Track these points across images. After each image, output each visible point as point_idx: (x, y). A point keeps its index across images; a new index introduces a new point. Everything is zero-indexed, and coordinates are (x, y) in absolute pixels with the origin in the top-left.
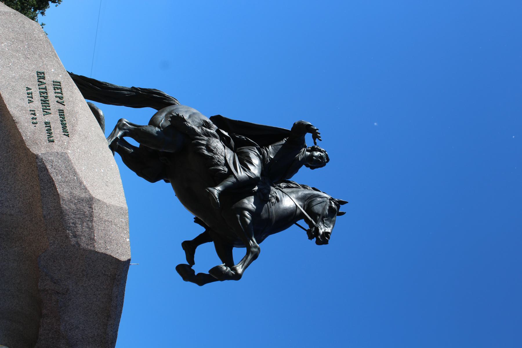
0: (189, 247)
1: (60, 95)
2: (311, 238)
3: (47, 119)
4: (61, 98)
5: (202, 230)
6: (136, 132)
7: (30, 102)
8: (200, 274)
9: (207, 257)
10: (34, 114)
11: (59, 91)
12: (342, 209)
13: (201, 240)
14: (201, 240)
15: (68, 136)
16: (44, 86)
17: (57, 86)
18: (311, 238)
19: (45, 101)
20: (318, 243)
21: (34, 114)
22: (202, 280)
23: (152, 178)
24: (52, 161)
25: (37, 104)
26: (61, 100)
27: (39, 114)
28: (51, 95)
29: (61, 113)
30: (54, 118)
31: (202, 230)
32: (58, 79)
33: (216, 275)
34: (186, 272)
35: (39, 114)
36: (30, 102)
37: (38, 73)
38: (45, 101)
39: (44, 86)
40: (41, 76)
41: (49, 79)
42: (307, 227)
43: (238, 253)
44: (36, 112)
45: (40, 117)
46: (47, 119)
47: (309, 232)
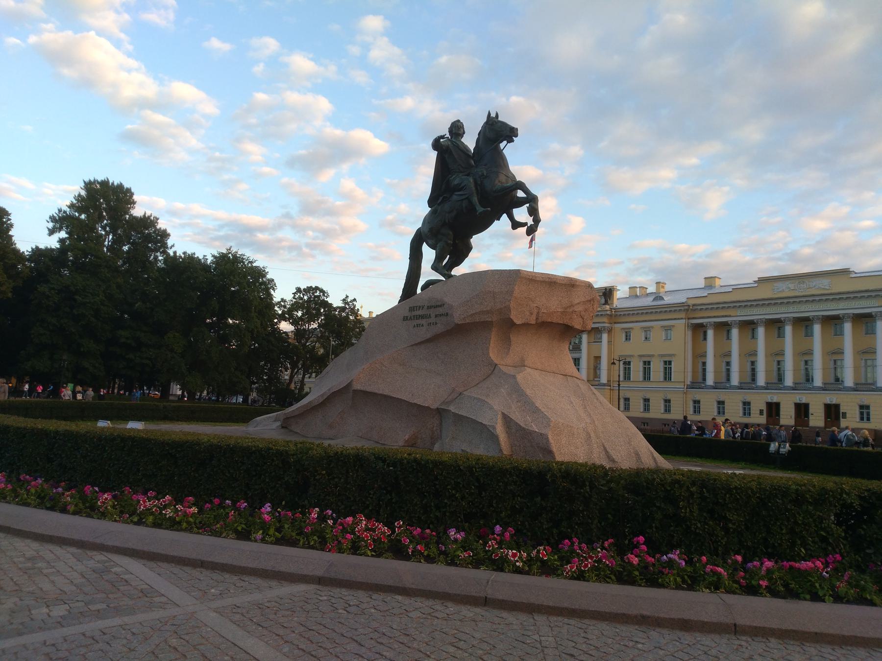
0: (516, 225)
2: (513, 141)
3: (433, 315)
5: (505, 215)
6: (439, 258)
9: (521, 214)
12: (493, 115)
13: (511, 217)
14: (511, 217)
17: (412, 309)
18: (513, 141)
19: (422, 317)
20: (516, 136)
22: (537, 221)
23: (469, 248)
25: (423, 322)
26: (421, 307)
30: (432, 312)
31: (505, 215)
33: (533, 212)
38: (422, 317)
40: (405, 319)
42: (505, 142)
43: (520, 194)
45: (433, 320)
46: (433, 315)
47: (508, 142)
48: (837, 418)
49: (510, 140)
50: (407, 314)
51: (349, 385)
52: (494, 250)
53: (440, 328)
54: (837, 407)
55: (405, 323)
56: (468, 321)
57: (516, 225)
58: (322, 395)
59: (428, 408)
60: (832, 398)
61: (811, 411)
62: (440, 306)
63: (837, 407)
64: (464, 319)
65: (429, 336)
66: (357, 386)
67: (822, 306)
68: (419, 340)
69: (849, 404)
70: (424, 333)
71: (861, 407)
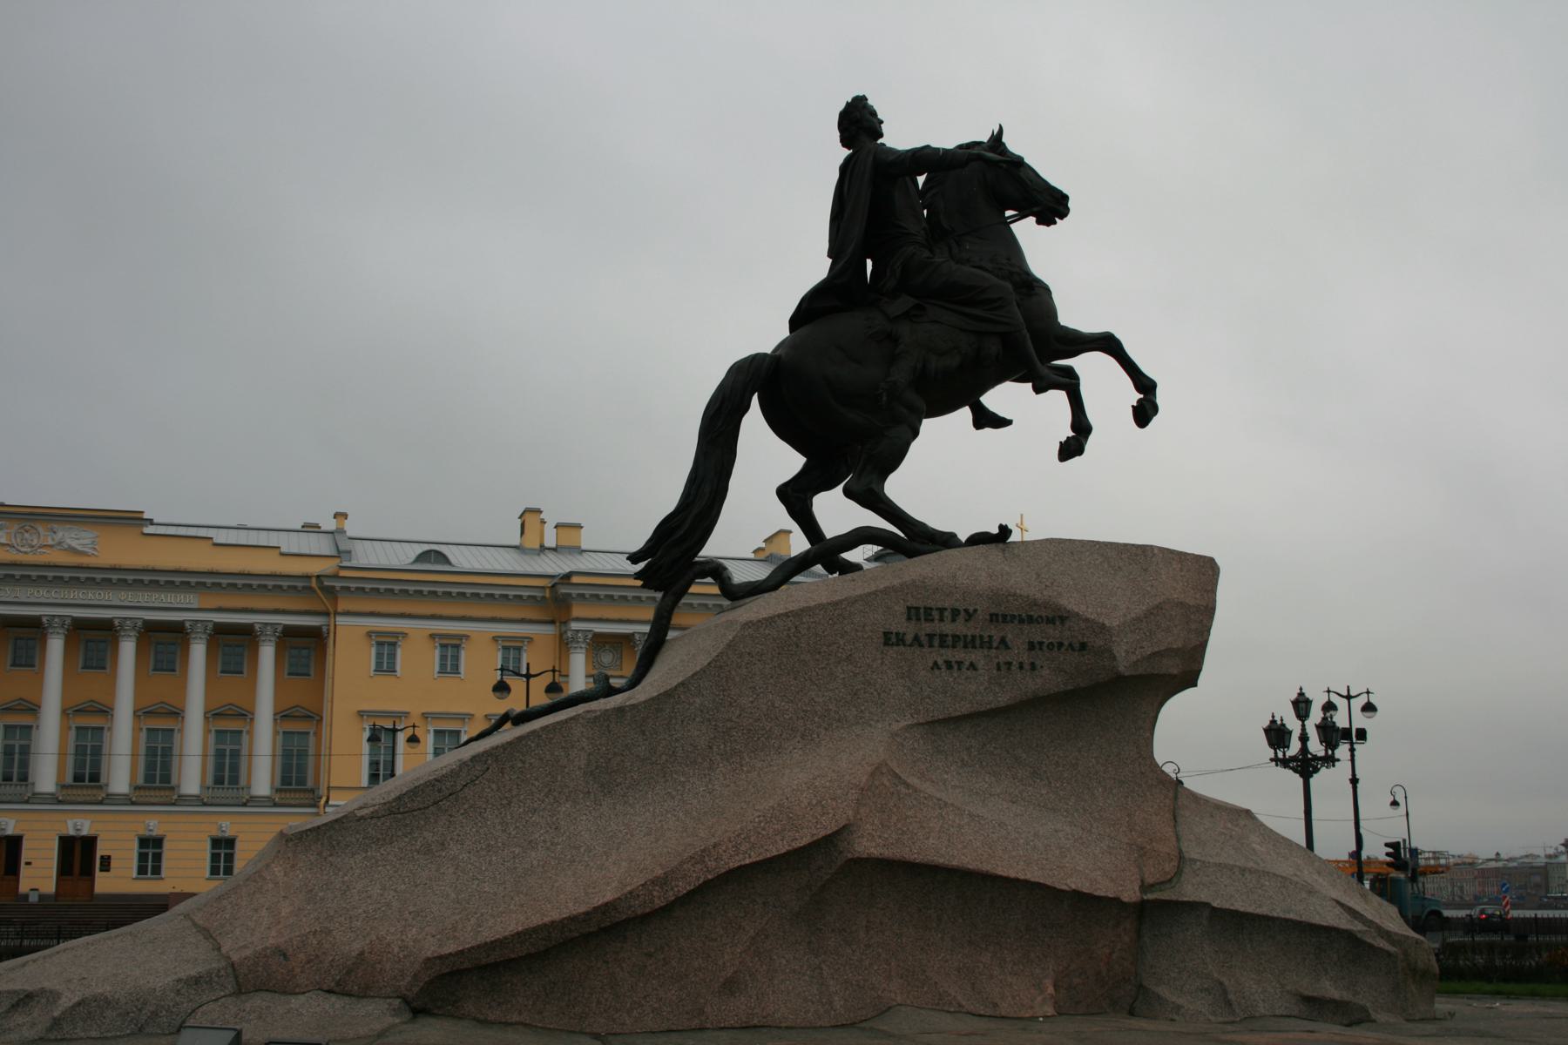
1: (946, 614)
4: (955, 613)
7: (972, 666)
8: (1073, 427)
10: (1009, 664)
11: (936, 614)
15: (1063, 619)
16: (924, 639)
21: (1009, 664)
24: (1127, 652)
25: (976, 656)
27: (1004, 657)
28: (948, 628)
29: (994, 618)
32: (900, 608)
34: (1071, 449)
35: (1004, 657)
36: (972, 666)
37: (886, 644)
38: (970, 643)
39: (924, 639)
41: (899, 624)
44: (1001, 659)
48: (88, 872)
49: (1046, 219)
50: (909, 630)
51: (827, 843)
52: (956, 472)
53: (1047, 679)
54: (89, 843)
55: (892, 652)
56: (1141, 671)
57: (985, 419)
58: (662, 882)
59: (1116, 901)
60: (81, 824)
61: (25, 855)
62: (1051, 621)
63: (89, 843)
64: (1135, 663)
65: (1003, 699)
66: (867, 845)
67: (144, 598)
68: (964, 708)
69: (118, 840)
70: (979, 688)
71: (144, 842)
